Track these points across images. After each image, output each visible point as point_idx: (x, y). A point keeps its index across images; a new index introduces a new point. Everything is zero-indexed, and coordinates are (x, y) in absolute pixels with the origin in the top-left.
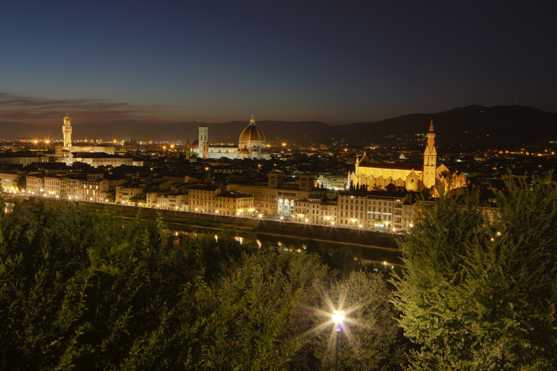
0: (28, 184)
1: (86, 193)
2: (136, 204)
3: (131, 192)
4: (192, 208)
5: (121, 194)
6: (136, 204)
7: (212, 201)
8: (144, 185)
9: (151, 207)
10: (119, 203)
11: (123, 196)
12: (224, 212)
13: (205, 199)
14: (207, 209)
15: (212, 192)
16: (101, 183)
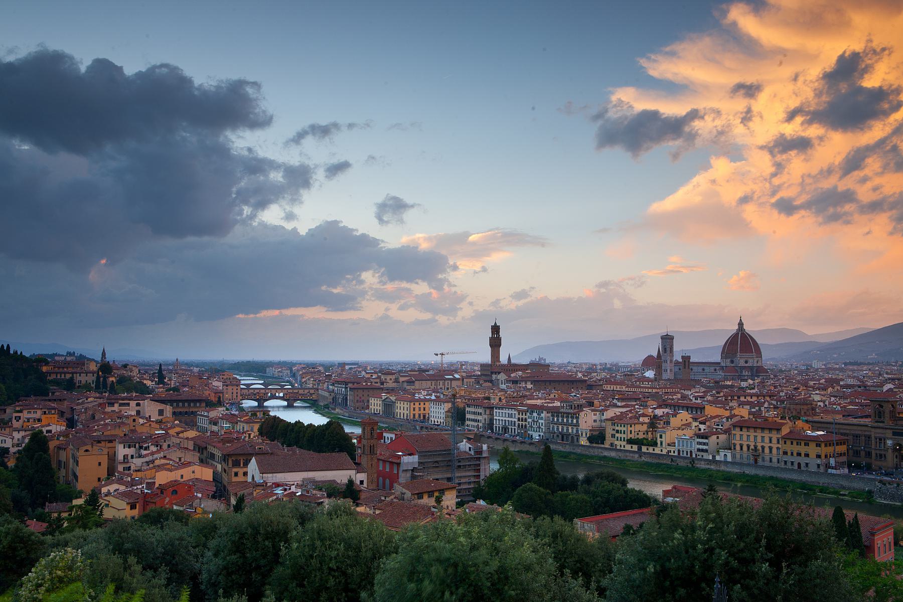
0: (468, 416)
1: (558, 429)
2: (640, 449)
3: (630, 429)
4: (738, 456)
5: (614, 432)
6: (640, 449)
7: (775, 446)
8: (646, 420)
10: (612, 444)
11: (617, 435)
12: (799, 464)
13: (763, 441)
14: (767, 458)
15: (775, 432)
16: (582, 414)
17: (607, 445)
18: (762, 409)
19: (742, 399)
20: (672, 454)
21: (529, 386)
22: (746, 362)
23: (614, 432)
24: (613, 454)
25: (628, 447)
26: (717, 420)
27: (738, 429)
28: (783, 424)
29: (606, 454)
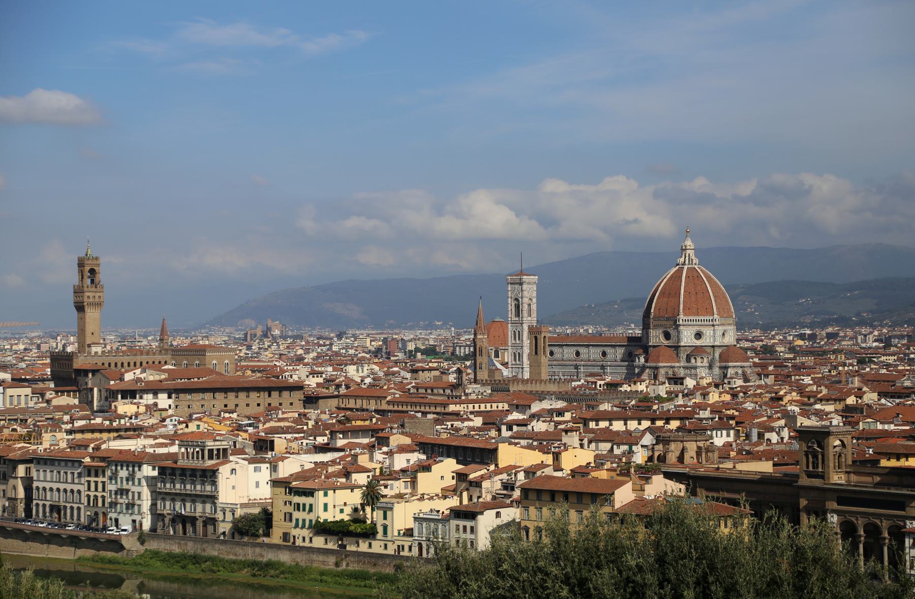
5: (289, 509)
9: (391, 551)
11: (296, 515)
16: (224, 471)
17: (276, 538)
18: (634, 448)
19: (618, 426)
20: (406, 553)
21: (163, 401)
22: (699, 335)
23: (289, 509)
24: (285, 557)
25: (319, 542)
26: (504, 476)
27: (532, 496)
28: (622, 484)
29: (270, 556)
